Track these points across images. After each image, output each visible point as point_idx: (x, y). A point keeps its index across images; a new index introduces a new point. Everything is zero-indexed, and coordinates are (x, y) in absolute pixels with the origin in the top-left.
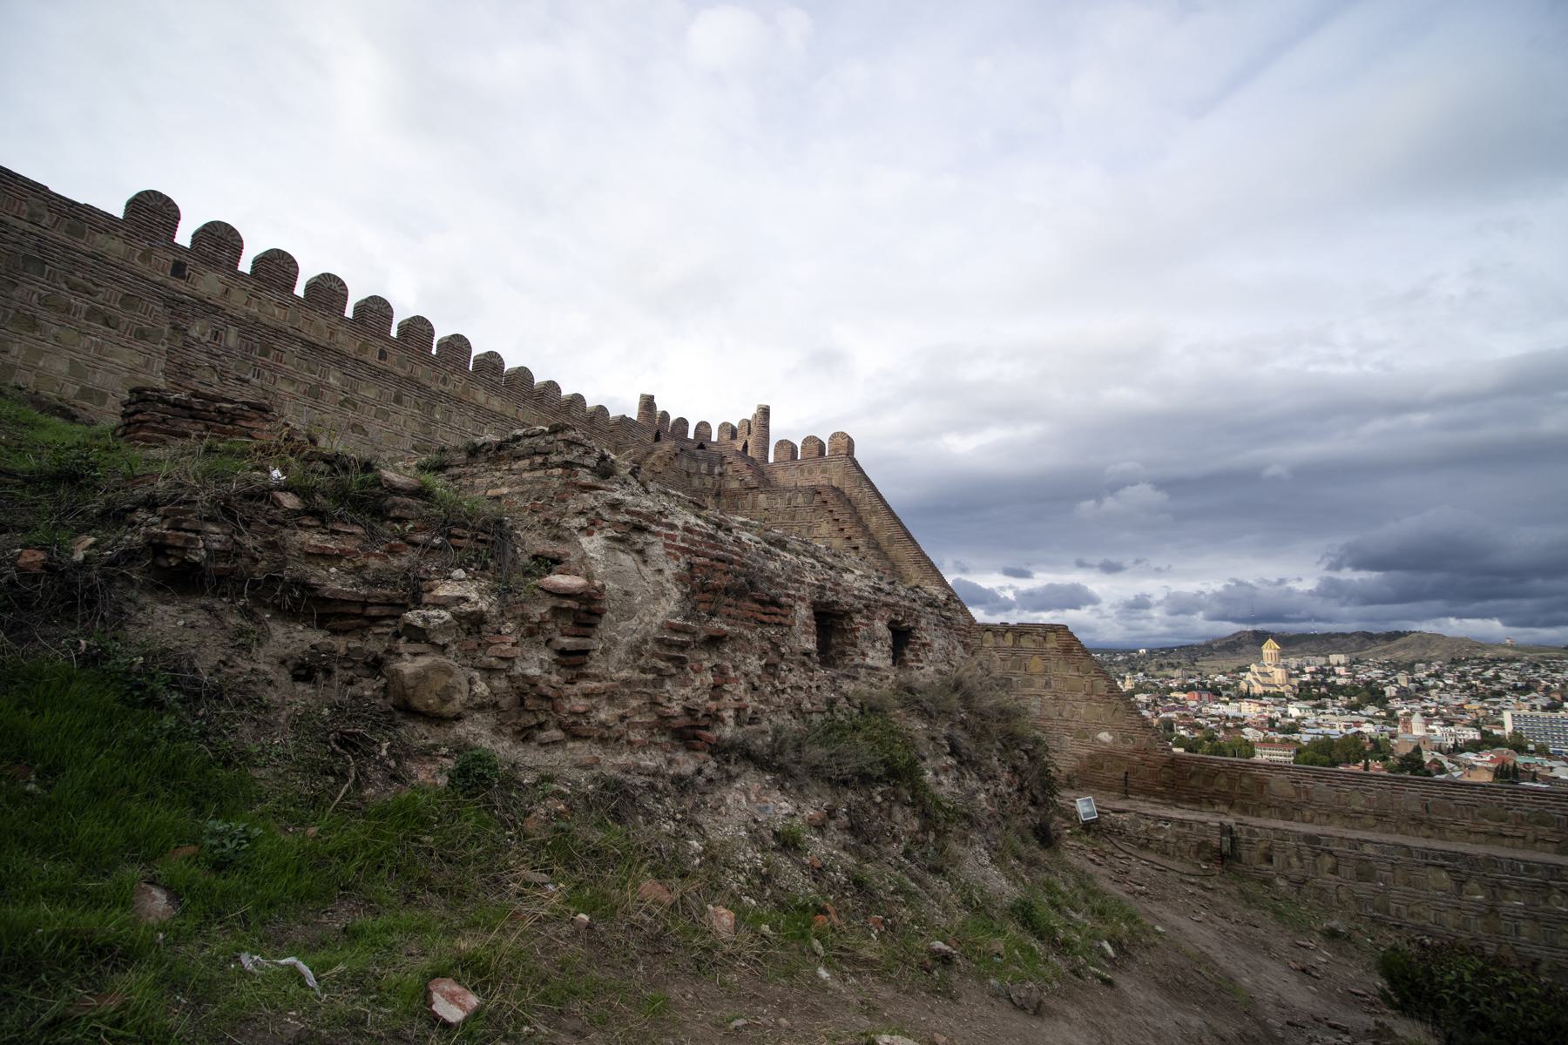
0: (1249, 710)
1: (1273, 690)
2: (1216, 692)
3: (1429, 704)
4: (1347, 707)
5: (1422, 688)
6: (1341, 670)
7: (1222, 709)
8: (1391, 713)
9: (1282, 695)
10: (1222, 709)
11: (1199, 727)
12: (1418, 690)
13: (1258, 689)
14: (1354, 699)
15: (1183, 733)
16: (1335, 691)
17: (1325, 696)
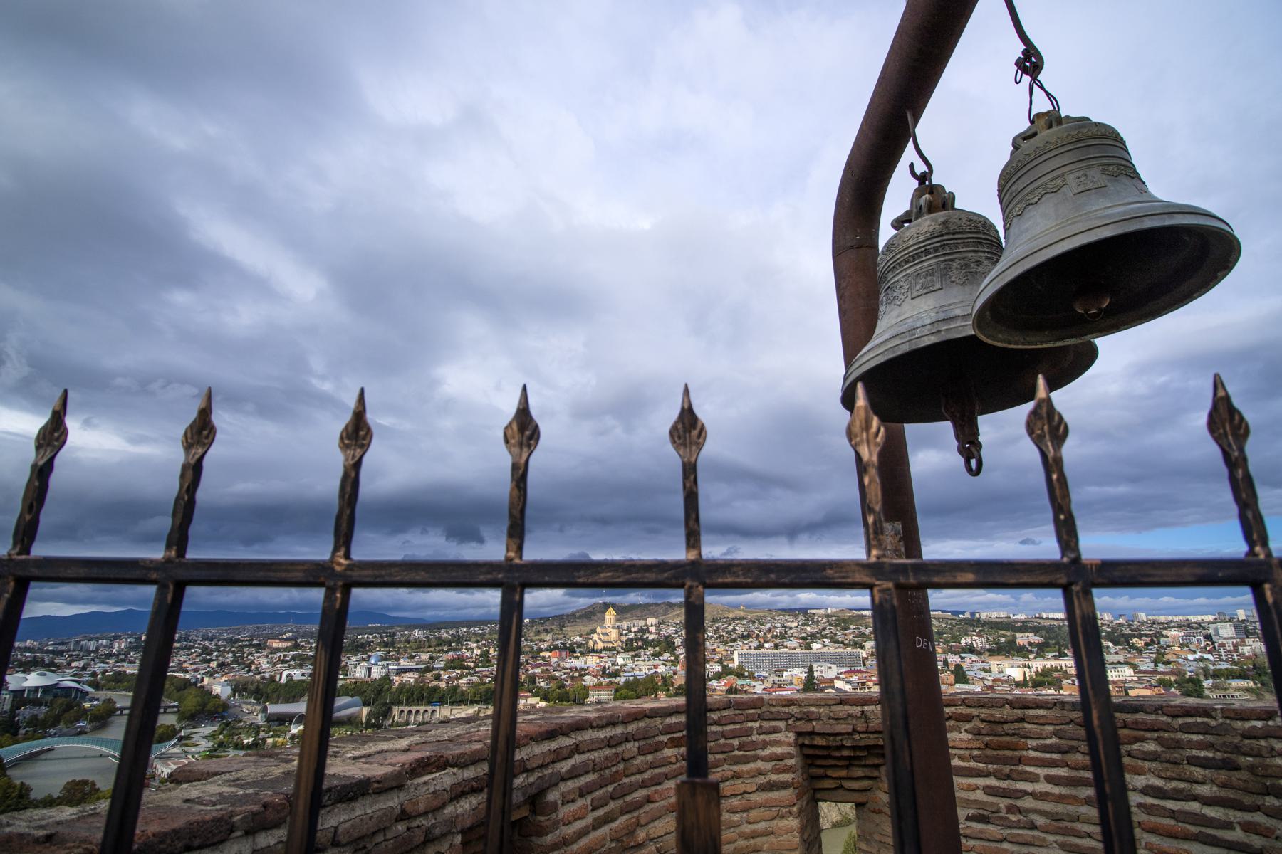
0: (592, 662)
2: (571, 650)
6: (652, 629)
9: (614, 649)
11: (554, 678)
13: (600, 646)
15: (542, 684)
16: (647, 643)
17: (640, 648)
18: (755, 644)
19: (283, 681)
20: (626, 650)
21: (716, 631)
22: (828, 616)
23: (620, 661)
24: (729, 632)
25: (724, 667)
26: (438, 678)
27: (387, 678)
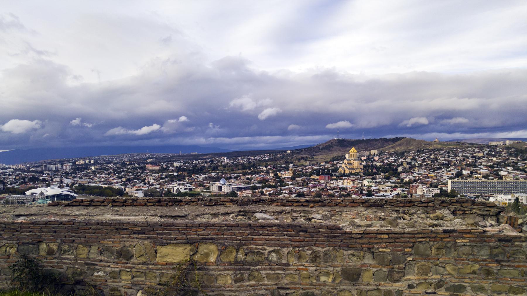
0: (347, 183)
1: (353, 171)
2: (329, 173)
3: (416, 175)
4: (384, 178)
5: (412, 167)
6: (376, 158)
7: (335, 184)
8: (402, 180)
9: (358, 174)
10: (335, 184)
12: (410, 168)
13: (347, 171)
14: (387, 174)
16: (379, 170)
17: (375, 173)
18: (455, 171)
19: (175, 192)
20: (367, 174)
21: (424, 161)
22: (508, 148)
23: (366, 183)
24: (432, 161)
25: (441, 190)
26: (262, 193)
27: (233, 194)
